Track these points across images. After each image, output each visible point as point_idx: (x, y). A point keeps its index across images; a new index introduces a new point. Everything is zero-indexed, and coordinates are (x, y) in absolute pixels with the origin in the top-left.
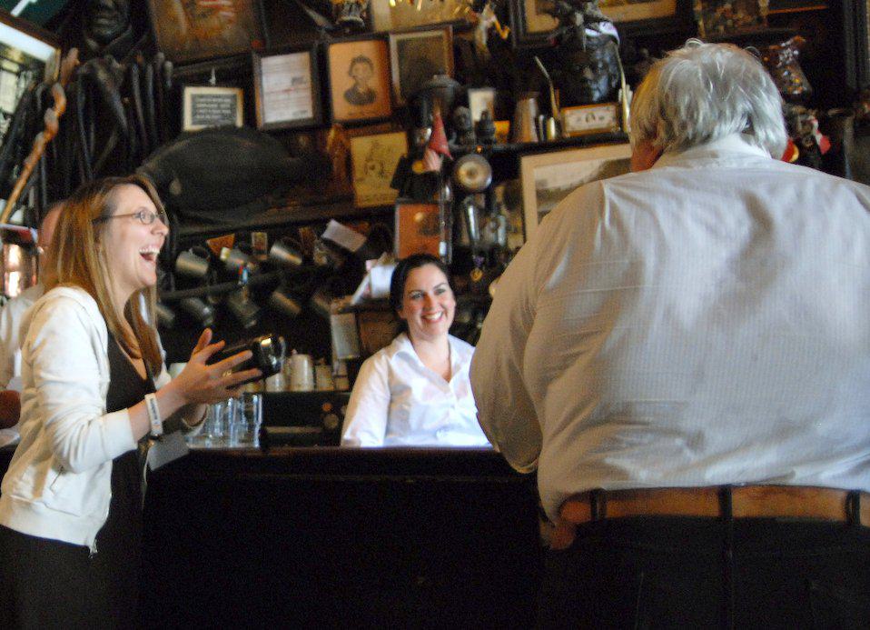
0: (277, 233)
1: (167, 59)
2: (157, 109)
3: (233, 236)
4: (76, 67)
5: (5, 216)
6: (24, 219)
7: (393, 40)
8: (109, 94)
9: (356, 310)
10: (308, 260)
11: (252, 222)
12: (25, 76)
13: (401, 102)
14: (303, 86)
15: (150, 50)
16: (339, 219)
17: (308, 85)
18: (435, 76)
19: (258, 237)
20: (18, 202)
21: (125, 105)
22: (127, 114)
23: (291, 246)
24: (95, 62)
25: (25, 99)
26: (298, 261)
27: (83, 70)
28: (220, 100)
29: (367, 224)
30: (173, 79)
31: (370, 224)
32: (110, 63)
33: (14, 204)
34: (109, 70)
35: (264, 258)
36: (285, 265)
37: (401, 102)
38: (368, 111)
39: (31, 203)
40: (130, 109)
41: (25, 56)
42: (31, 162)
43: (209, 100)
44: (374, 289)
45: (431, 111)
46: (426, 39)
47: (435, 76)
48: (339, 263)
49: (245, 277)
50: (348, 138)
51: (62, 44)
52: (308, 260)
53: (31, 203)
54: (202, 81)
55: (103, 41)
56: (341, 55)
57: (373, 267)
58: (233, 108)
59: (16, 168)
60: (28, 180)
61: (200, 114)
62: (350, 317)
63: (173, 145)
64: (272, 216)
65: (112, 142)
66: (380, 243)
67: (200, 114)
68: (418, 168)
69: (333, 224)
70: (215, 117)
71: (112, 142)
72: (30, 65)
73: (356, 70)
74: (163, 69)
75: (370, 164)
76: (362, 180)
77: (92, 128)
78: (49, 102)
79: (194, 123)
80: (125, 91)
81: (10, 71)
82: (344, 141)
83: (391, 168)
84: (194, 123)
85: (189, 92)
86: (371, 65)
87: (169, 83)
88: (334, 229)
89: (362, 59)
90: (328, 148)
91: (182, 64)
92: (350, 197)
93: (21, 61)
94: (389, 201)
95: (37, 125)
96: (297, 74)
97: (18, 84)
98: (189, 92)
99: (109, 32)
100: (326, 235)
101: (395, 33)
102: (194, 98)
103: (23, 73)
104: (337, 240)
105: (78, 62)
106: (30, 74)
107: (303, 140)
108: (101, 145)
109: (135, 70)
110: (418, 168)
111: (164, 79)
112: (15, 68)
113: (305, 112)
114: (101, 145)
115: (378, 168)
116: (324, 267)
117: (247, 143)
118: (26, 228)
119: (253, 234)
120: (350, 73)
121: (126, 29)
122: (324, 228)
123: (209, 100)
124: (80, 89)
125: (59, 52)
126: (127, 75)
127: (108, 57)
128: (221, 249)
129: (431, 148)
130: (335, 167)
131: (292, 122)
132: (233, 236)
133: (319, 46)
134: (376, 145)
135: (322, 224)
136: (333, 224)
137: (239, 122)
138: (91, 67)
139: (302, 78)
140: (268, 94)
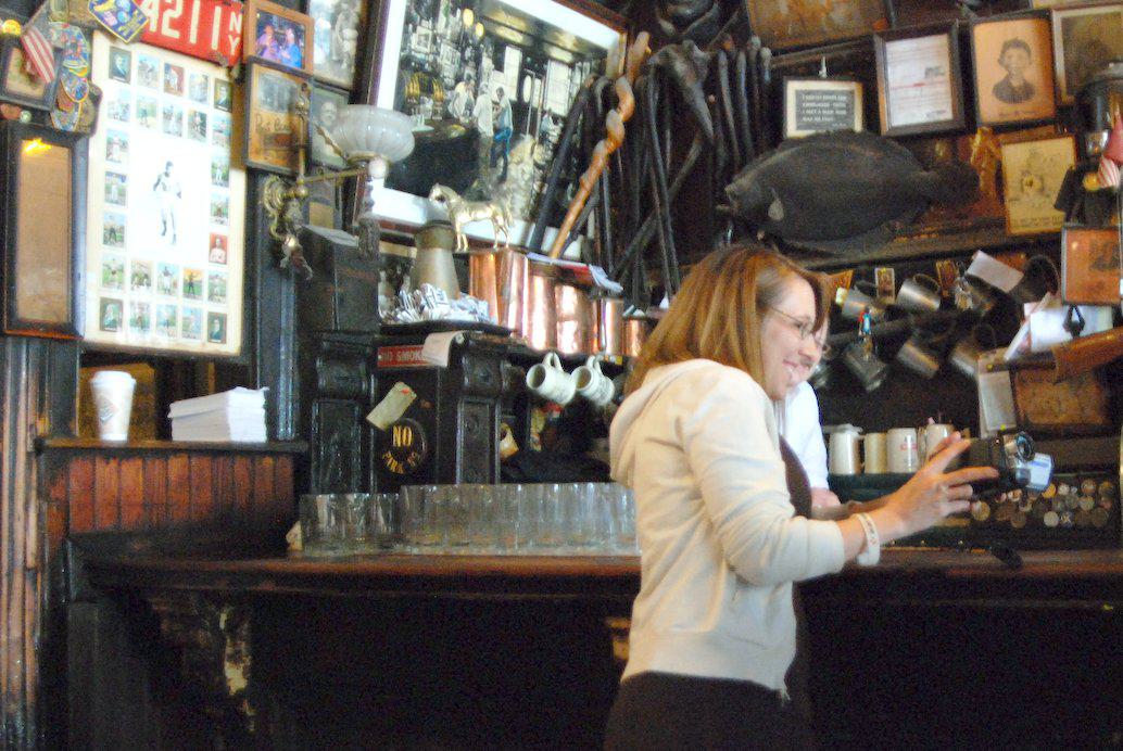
0: (910, 268)
1: (763, 45)
2: (751, 105)
3: (850, 273)
4: (647, 56)
7: (1057, 18)
8: (689, 91)
9: (1013, 368)
10: (948, 303)
11: (876, 255)
12: (581, 69)
13: (1067, 98)
14: (940, 78)
15: (742, 33)
16: (989, 251)
17: (947, 77)
18: (1111, 65)
19: (884, 274)
21: (711, 106)
22: (713, 118)
23: (927, 286)
24: (670, 49)
25: (583, 98)
26: (935, 304)
27: (656, 60)
28: (833, 97)
29: (1023, 256)
30: (773, 72)
31: (1028, 256)
32: (691, 48)
33: (568, 234)
34: (689, 58)
35: (890, 300)
36: (918, 311)
37: (1067, 98)
38: (1023, 111)
39: (591, 232)
40: (716, 108)
41: (579, 41)
42: (589, 179)
43: (818, 98)
44: (1034, 341)
45: (1106, 109)
46: (1098, 16)
47: (1111, 65)
48: (988, 307)
50: (998, 146)
51: (628, 28)
52: (948, 303)
53: (591, 232)
54: (810, 72)
55: (681, 22)
56: (989, 37)
57: (1032, 312)
58: (849, 108)
59: (571, 187)
61: (808, 116)
62: (1004, 376)
63: (773, 153)
64: (901, 247)
65: (694, 153)
66: (1042, 279)
67: (808, 116)
68: (1091, 183)
69: (980, 256)
70: (828, 120)
71: (694, 153)
72: (588, 54)
73: (1010, 57)
74: (759, 57)
75: (1027, 179)
76: (1016, 199)
77: (668, 134)
78: (611, 101)
79: (799, 128)
80: (711, 86)
81: (561, 62)
82: (993, 149)
83: (1056, 184)
84: (799, 128)
85: (793, 88)
86: (1029, 52)
87: (767, 77)
88: (981, 263)
89: (1017, 44)
90: (972, 159)
91: (785, 51)
92: (1001, 223)
93: (576, 49)
94: (1051, 227)
95: (597, 131)
96: (932, 64)
97: (571, 78)
98: (793, 88)
99: (688, 12)
100: (971, 271)
101: (1058, 9)
102: (799, 94)
103: (580, 64)
104: (985, 278)
105: (649, 50)
106: (587, 65)
107: (940, 149)
108: (680, 154)
109: (723, 60)
110: (1091, 183)
111: (760, 72)
112: (568, 58)
113: (940, 112)
114: (680, 154)
115: (1037, 183)
116: (969, 311)
117: (869, 153)
118: (583, 265)
119: (877, 270)
120: (1000, 62)
121: (710, 8)
122: (969, 262)
123: (818, 98)
124: (651, 86)
125: (625, 37)
126: (713, 65)
127: (687, 43)
129: (1108, 157)
130: (982, 183)
131: (926, 125)
132: (850, 273)
133: (961, 26)
134: (1034, 155)
135: (965, 257)
136: (980, 256)
137: (858, 126)
138: (667, 55)
139: (937, 68)
140: (895, 89)
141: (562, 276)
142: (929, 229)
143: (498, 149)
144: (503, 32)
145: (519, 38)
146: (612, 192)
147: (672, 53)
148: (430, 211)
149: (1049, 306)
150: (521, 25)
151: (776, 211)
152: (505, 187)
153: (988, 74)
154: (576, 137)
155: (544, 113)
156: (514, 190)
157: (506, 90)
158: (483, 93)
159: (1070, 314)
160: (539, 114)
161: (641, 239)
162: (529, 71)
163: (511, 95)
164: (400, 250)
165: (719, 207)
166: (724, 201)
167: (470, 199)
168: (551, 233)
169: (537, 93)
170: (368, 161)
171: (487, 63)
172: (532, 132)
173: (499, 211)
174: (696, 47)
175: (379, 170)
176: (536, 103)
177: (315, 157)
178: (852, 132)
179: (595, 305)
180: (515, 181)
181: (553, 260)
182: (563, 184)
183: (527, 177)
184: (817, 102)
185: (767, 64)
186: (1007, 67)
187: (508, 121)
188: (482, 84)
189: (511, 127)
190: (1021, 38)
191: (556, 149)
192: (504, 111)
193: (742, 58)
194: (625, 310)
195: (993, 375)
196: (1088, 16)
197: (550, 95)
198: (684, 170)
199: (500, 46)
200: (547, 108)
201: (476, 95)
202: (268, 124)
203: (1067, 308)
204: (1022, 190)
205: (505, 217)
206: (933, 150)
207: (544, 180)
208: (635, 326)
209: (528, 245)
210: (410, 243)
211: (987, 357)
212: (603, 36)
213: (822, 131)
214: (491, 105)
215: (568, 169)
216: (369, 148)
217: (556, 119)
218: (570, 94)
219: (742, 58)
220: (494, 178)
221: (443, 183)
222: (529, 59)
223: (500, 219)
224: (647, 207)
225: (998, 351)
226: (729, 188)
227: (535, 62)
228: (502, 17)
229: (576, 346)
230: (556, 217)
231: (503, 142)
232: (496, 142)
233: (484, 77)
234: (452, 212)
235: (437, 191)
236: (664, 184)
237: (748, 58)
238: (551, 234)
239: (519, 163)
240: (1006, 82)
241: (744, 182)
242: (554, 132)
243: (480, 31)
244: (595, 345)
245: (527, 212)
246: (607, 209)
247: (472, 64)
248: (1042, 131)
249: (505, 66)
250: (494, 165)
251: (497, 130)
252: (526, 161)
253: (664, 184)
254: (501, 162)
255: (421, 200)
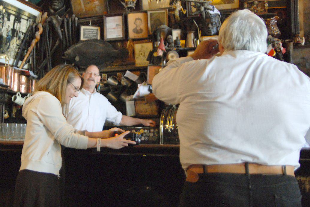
2: (72, 32)
4: (47, 18)
7: (149, 13)
9: (135, 100)
10: (120, 83)
12: (30, 21)
13: (151, 33)
14: (120, 27)
15: (71, 13)
16: (130, 71)
17: (121, 27)
18: (162, 25)
21: (62, 32)
22: (62, 34)
23: (115, 79)
24: (52, 17)
25: (29, 28)
26: (116, 83)
27: (49, 19)
28: (93, 31)
29: (139, 72)
31: (140, 72)
32: (57, 17)
34: (57, 19)
35: (105, 82)
36: (112, 85)
37: (151, 33)
38: (140, 36)
39: (31, 62)
40: (63, 32)
41: (29, 14)
42: (30, 49)
43: (89, 30)
44: (140, 93)
47: (162, 25)
48: (129, 85)
50: (134, 44)
51: (42, 11)
53: (31, 62)
54: (87, 24)
55: (55, 10)
56: (132, 17)
57: (140, 86)
58: (97, 34)
59: (26, 51)
61: (86, 35)
62: (133, 102)
63: (77, 44)
65: (57, 43)
66: (143, 78)
68: (155, 54)
69: (128, 72)
70: (91, 36)
71: (57, 43)
73: (137, 22)
74: (75, 20)
75: (140, 53)
76: (138, 58)
78: (37, 29)
79: (84, 38)
80: (62, 27)
81: (25, 19)
82: (132, 45)
83: (147, 54)
84: (84, 38)
85: (83, 28)
87: (76, 25)
89: (139, 19)
90: (127, 47)
92: (134, 64)
93: (28, 16)
94: (146, 65)
95: (33, 37)
97: (27, 23)
98: (83, 28)
99: (57, 7)
100: (126, 75)
101: (149, 11)
102: (84, 29)
103: (29, 20)
104: (129, 77)
105: (47, 17)
106: (31, 20)
107: (119, 44)
108: (54, 44)
109: (65, 20)
110: (155, 54)
111: (75, 24)
112: (26, 18)
113: (119, 35)
114: (54, 44)
115: (143, 54)
117: (101, 45)
120: (134, 23)
122: (125, 73)
123: (89, 30)
125: (41, 13)
126: (63, 21)
129: (159, 48)
130: (129, 53)
134: (142, 47)
135: (124, 72)
136: (128, 72)
137: (99, 38)
138: (51, 18)
141: (22, 73)
142: (115, 64)
143: (8, 40)
144: (10, 11)
145: (14, 13)
146: (36, 52)
147: (53, 18)
149: (144, 85)
150: (15, 10)
151: (77, 59)
152: (9, 50)
153: (131, 27)
154: (27, 38)
155: (20, 32)
157: (10, 26)
158: (4, 26)
159: (150, 87)
160: (18, 32)
161: (43, 64)
162: (16, 21)
163: (11, 27)
165: (63, 57)
166: (64, 55)
168: (20, 62)
169: (18, 27)
171: (6, 19)
172: (16, 37)
173: (7, 56)
174: (59, 17)
176: (18, 29)
178: (97, 39)
179: (30, 81)
180: (12, 49)
181: (20, 69)
182: (24, 50)
183: (15, 48)
184: (88, 31)
185: (76, 21)
186: (136, 25)
187: (10, 33)
188: (4, 24)
189: (11, 35)
190: (140, 17)
191: (22, 41)
192: (9, 31)
193: (70, 20)
195: (130, 102)
196: (156, 13)
197: (21, 27)
198: (55, 47)
199: (9, 15)
200: (20, 31)
201: (2, 27)
203: (149, 85)
204: (139, 55)
205: (8, 58)
206: (117, 44)
207: (19, 49)
209: (14, 65)
211: (128, 97)
212: (35, 12)
213: (90, 39)
214: (6, 29)
215: (25, 46)
217: (23, 33)
218: (27, 27)
219: (70, 20)
220: (6, 48)
222: (16, 18)
223: (7, 59)
224: (45, 57)
225: (132, 96)
226: (66, 52)
227: (18, 19)
228: (10, 8)
229: (25, 91)
230: (22, 58)
231: (9, 39)
232: (7, 39)
233: (5, 22)
236: (49, 50)
237: (72, 19)
238: (20, 62)
239: (13, 44)
240: (136, 28)
241: (69, 51)
242: (22, 37)
243: (4, 11)
245: (14, 57)
246: (35, 57)
247: (2, 19)
248: (144, 41)
249: (10, 20)
250: (6, 44)
251: (7, 36)
252: (15, 44)
253: (49, 50)
254: (8, 44)
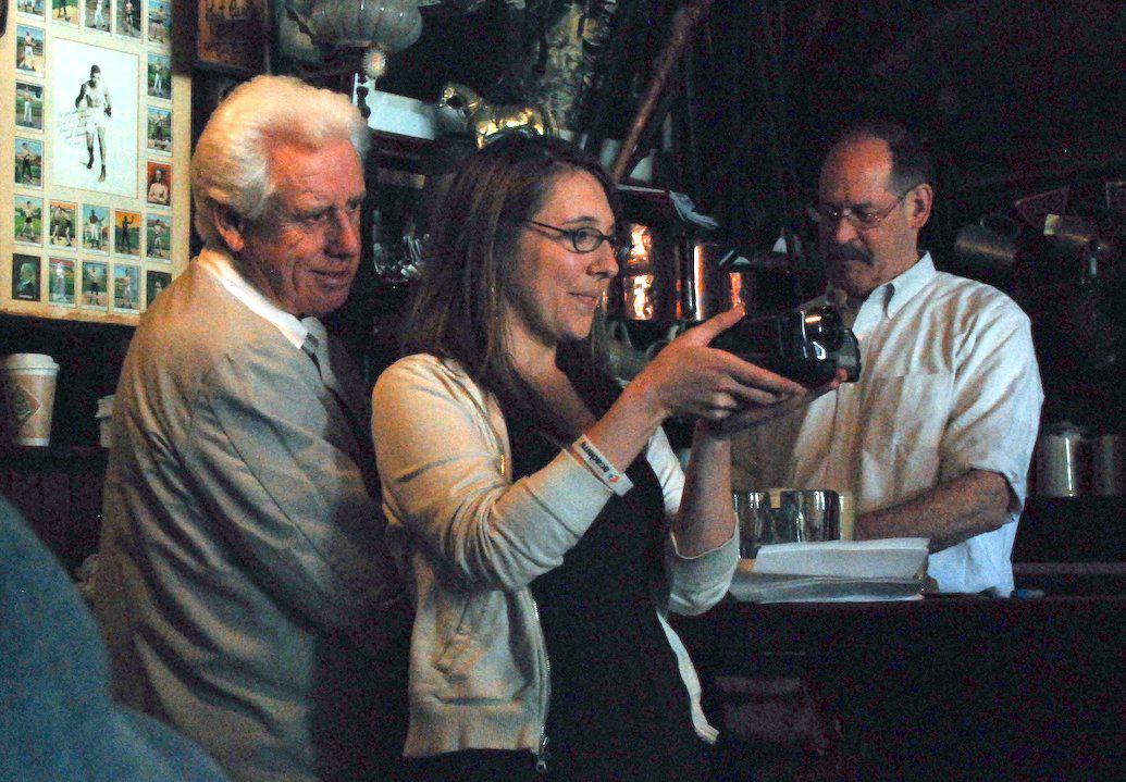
3: (1064, 190)
5: (619, 170)
6: (655, 170)
20: (640, 142)
39: (667, 141)
42: (664, 66)
49: (1094, 270)
53: (667, 141)
60: (661, 95)
128: (1044, 216)
148: (440, 123)
152: (543, 82)
156: (556, 87)
164: (398, 177)
167: (492, 102)
170: (362, 52)
173: (538, 116)
175: (376, 64)
177: (284, 50)
179: (676, 251)
180: (558, 71)
183: (574, 65)
194: (722, 256)
202: (222, 8)
207: (598, 69)
208: (736, 279)
210: (414, 168)
216: (362, 35)
220: (528, 69)
221: (459, 80)
229: (649, 310)
234: (473, 120)
235: (449, 94)
239: (561, 46)
244: (678, 310)
250: (528, 50)
255: (428, 109)
